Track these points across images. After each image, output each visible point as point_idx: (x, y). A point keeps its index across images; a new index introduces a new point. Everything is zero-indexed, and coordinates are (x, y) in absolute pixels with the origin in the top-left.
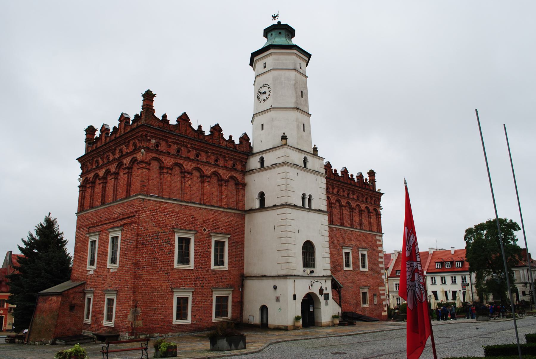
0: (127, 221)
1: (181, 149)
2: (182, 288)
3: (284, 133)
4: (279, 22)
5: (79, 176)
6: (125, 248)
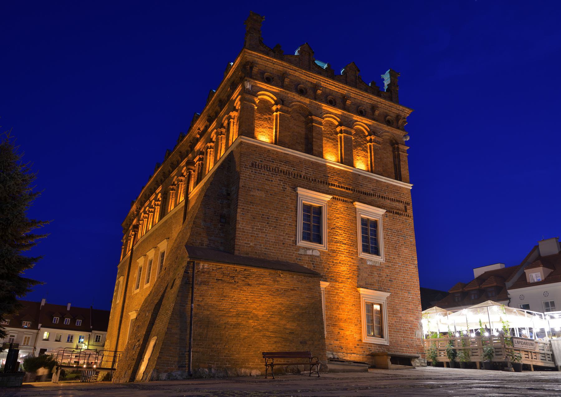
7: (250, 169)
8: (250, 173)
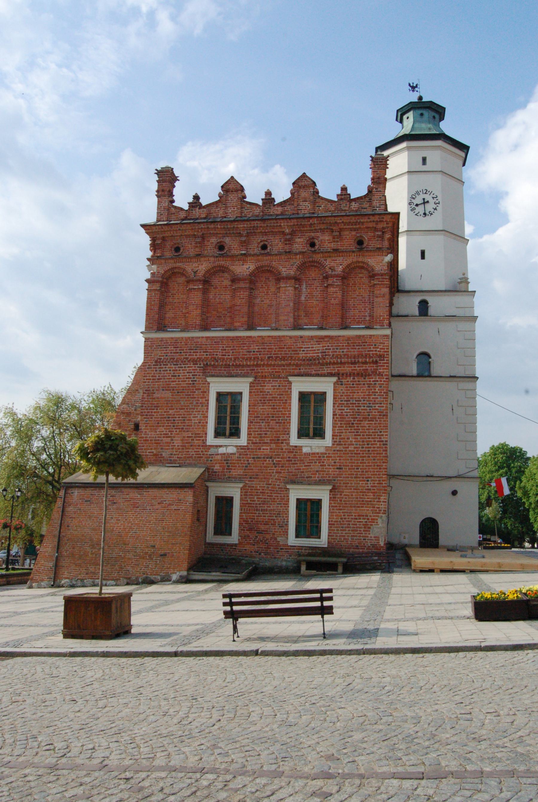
0: (347, 369)
4: (420, 98)
6: (350, 415)
7: (154, 368)
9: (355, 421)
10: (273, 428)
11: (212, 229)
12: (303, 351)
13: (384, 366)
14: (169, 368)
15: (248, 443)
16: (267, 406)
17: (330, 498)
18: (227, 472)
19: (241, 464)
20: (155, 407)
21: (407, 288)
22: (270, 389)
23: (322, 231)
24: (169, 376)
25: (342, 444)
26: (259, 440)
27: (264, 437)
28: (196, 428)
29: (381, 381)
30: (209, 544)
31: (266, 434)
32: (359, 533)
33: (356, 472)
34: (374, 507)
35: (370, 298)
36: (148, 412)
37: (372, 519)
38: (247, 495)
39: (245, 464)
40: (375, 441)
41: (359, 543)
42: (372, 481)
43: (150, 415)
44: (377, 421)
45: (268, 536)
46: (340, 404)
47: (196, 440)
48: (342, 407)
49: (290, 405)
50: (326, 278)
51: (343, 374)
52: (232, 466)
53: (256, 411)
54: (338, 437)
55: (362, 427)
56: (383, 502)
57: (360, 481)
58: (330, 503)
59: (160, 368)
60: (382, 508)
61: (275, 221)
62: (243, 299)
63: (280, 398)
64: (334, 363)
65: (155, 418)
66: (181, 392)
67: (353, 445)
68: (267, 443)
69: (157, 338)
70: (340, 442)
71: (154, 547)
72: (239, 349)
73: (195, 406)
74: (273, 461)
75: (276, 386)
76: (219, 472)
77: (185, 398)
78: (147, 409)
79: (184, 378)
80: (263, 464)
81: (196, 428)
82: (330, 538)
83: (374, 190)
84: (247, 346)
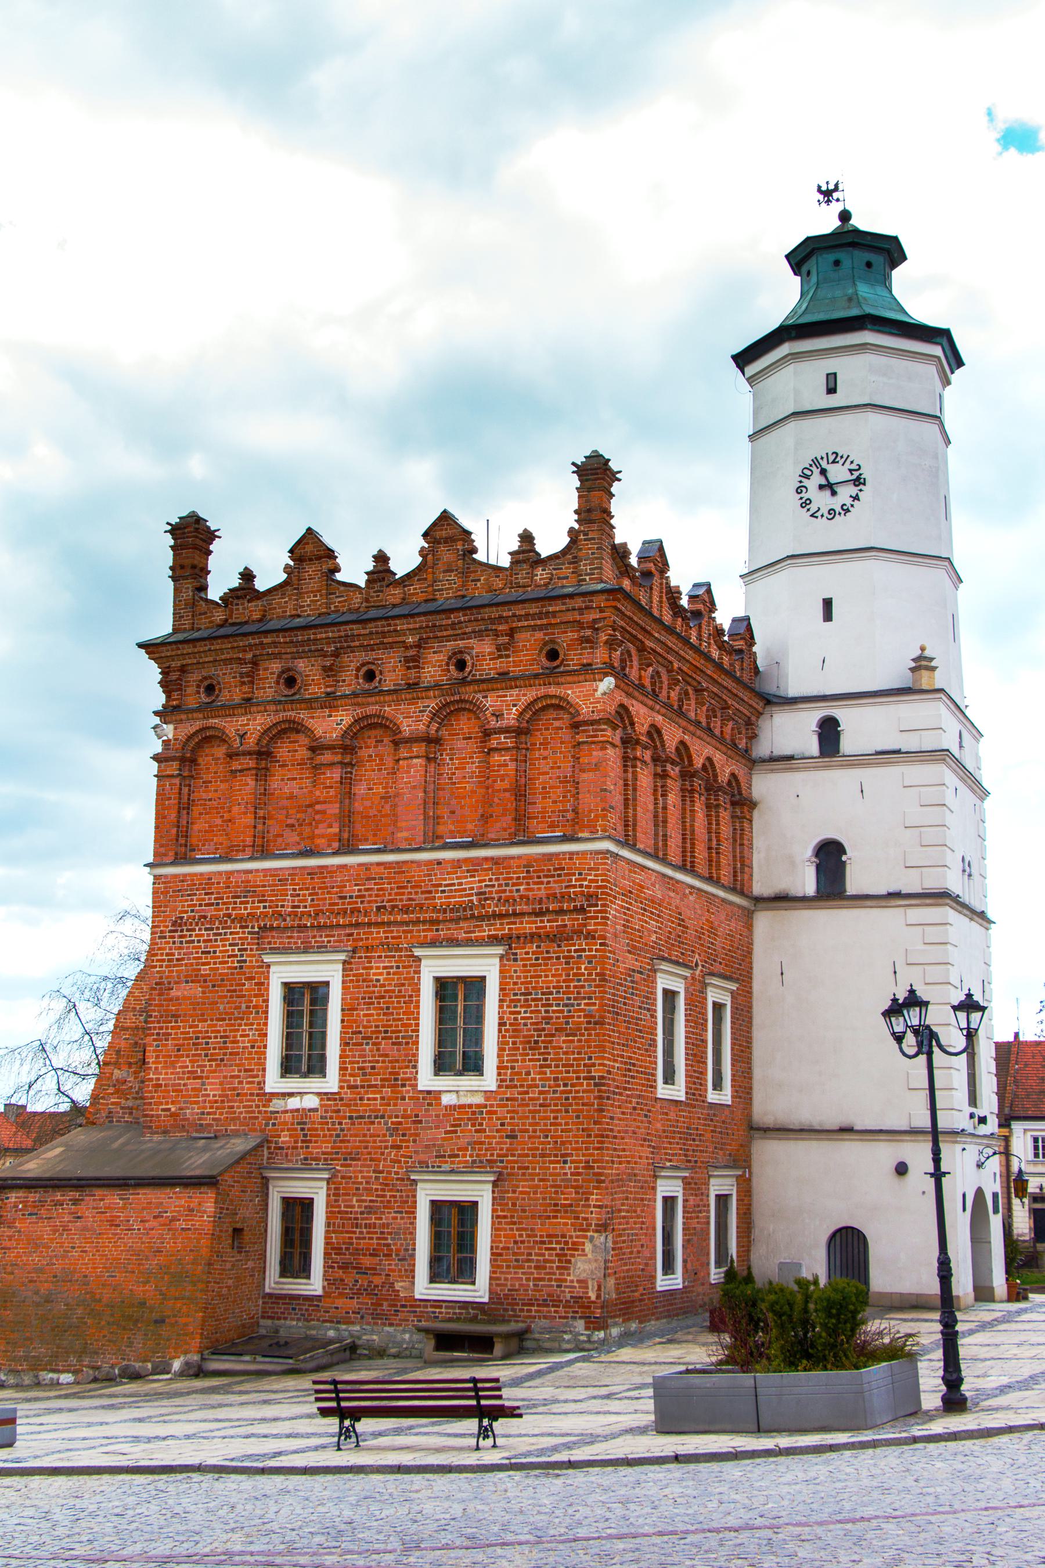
1: (660, 677)
2: (668, 1164)
3: (923, 649)
4: (845, 216)
5: (156, 713)
6: (532, 1024)
7: (171, 937)
8: (171, 949)
9: (539, 1036)
10: (387, 1055)
11: (269, 645)
12: (443, 892)
13: (597, 918)
14: (197, 936)
15: (341, 1087)
16: (375, 1009)
17: (494, 1198)
18: (302, 1148)
19: (329, 1130)
20: (174, 1016)
21: (792, 692)
22: (381, 974)
23: (479, 634)
24: (197, 953)
25: (516, 1086)
26: (362, 1081)
27: (370, 1074)
28: (246, 1059)
29: (590, 950)
30: (270, 1295)
31: (373, 1068)
32: (550, 1273)
33: (543, 1143)
34: (577, 1218)
35: (573, 772)
36: (161, 1028)
37: (574, 1243)
38: (338, 1195)
39: (335, 1130)
40: (578, 1078)
41: (549, 1295)
42: (572, 1162)
43: (164, 1034)
44: (582, 1035)
45: (377, 1280)
46: (511, 1001)
47: (248, 1083)
48: (515, 1006)
49: (418, 1007)
50: (487, 734)
51: (518, 938)
52: (311, 1135)
53: (355, 1021)
54: (509, 1071)
55: (554, 1048)
56: (595, 1206)
57: (551, 1162)
58: (494, 1210)
59: (181, 937)
60: (592, 1219)
61: (384, 623)
62: (331, 787)
63: (400, 991)
64: (501, 916)
65: (173, 1039)
66: (219, 986)
67: (537, 1086)
68: (376, 1086)
69: (176, 876)
70: (511, 1080)
71: (142, 1304)
72: (323, 893)
73: (244, 1013)
74: (386, 1123)
75: (392, 967)
76: (288, 1148)
77: (226, 997)
78: (159, 1022)
79: (223, 957)
80: (369, 1130)
81: (246, 1059)
82: (494, 1282)
83: (582, 537)
84: (338, 887)
